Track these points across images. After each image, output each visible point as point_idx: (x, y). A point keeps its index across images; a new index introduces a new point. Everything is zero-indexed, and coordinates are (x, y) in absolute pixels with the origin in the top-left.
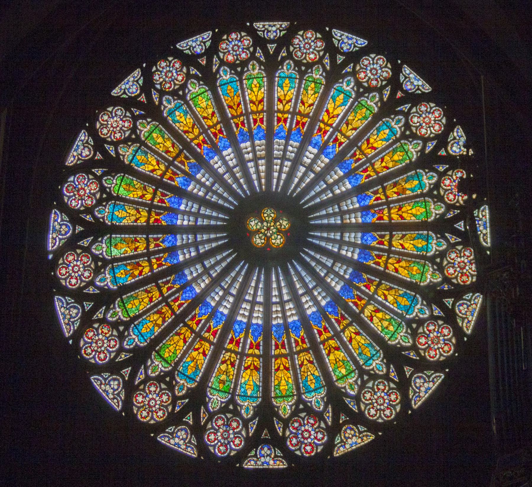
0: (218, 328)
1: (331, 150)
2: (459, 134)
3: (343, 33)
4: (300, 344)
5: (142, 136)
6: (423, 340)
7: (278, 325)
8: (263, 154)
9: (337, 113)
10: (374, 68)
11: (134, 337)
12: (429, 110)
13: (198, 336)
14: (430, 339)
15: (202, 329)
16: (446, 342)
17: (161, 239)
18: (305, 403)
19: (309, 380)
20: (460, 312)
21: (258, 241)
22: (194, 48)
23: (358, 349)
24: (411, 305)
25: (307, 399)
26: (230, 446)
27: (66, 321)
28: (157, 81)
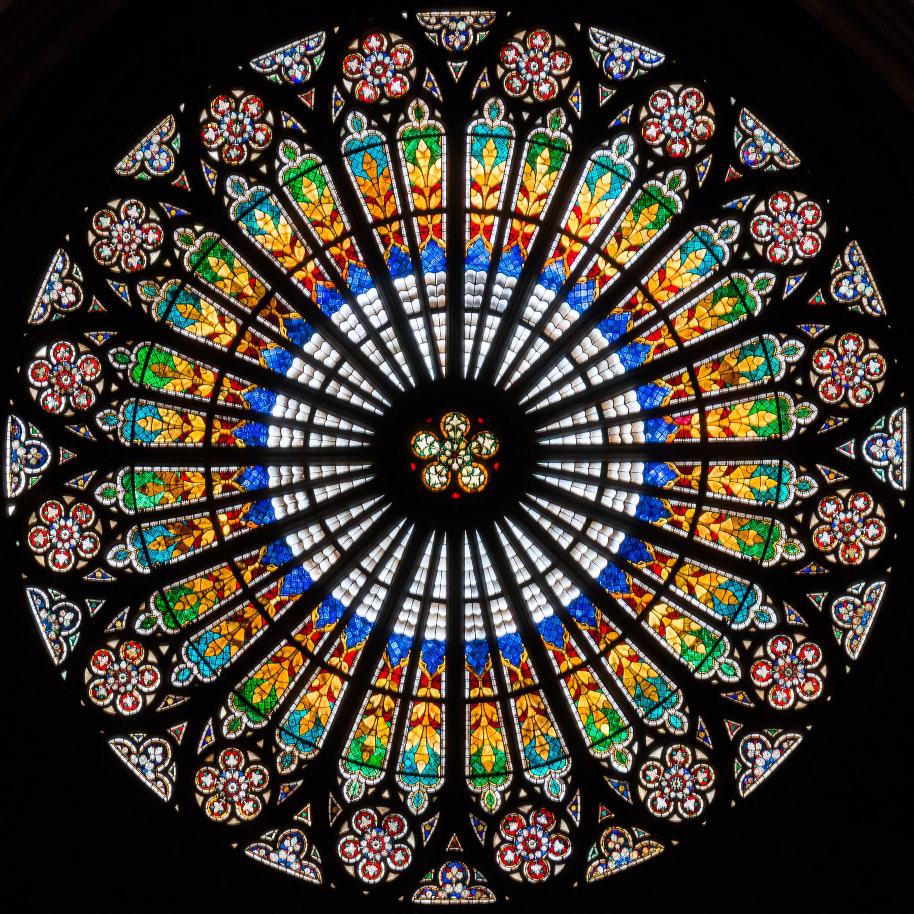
0: (358, 647)
1: (583, 293)
2: (855, 259)
3: (612, 36)
4: (521, 678)
5: (185, 262)
6: (763, 672)
7: (476, 643)
8: (442, 302)
9: (598, 214)
10: (677, 116)
11: (190, 665)
12: (792, 207)
13: (317, 662)
14: (777, 669)
15: (324, 650)
16: (809, 675)
17: (235, 476)
18: (529, 786)
19: (537, 744)
20: (840, 617)
22: (288, 69)
24: (741, 604)
25: (534, 781)
27: (53, 635)
28: (212, 142)
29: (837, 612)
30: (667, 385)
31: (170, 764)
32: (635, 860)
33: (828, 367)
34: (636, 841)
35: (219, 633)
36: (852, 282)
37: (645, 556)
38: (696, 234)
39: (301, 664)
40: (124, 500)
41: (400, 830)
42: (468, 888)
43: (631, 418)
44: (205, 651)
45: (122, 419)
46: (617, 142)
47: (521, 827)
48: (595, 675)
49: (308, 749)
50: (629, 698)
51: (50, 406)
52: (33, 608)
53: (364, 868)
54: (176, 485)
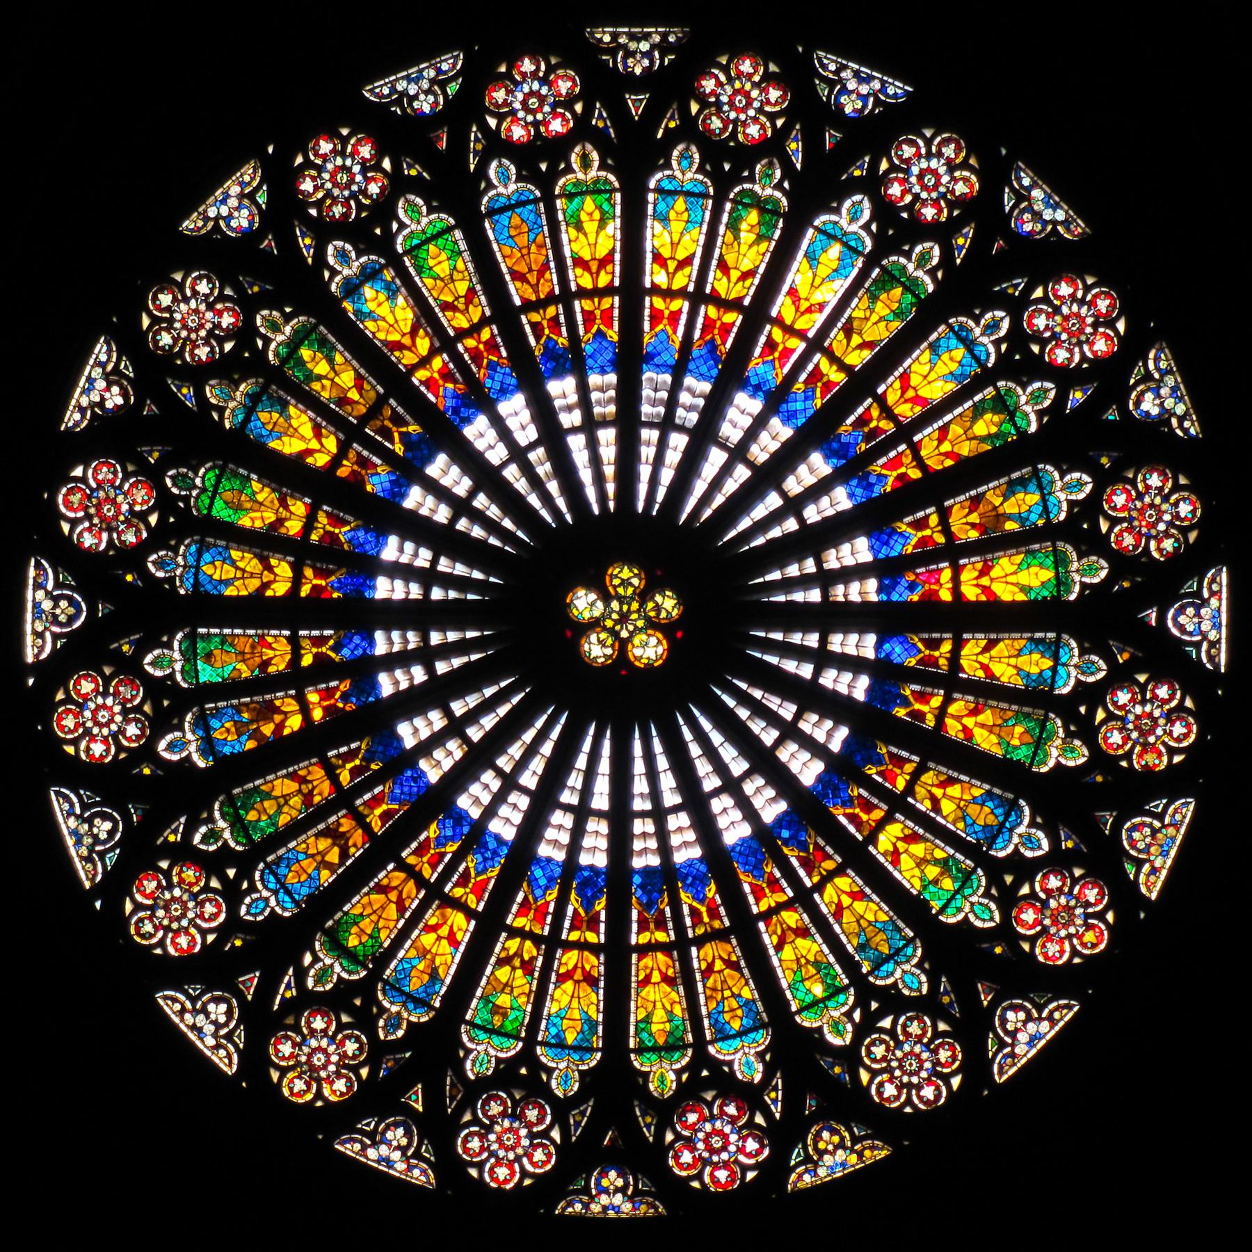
0: (489, 875)
1: (799, 406)
4: (706, 919)
5: (271, 356)
6: (1029, 916)
7: (647, 871)
9: (821, 300)
11: (265, 894)
12: (1080, 294)
13: (435, 894)
14: (1048, 913)
15: (445, 877)
16: (1090, 921)
17: (331, 642)
18: (715, 1064)
19: (726, 1009)
20: (1133, 844)
23: (858, 935)
24: (1002, 825)
25: (721, 1057)
27: (84, 851)
28: (310, 195)
29: (1130, 837)
30: (909, 530)
31: (237, 1027)
33: (1124, 508)
34: (855, 1140)
35: (305, 853)
36: (1158, 396)
37: (875, 757)
38: (951, 327)
39: (413, 895)
41: (541, 1120)
42: (631, 1199)
44: (286, 876)
45: (182, 563)
46: (848, 204)
47: (702, 1119)
48: (805, 916)
50: (850, 949)
51: (87, 545)
52: (59, 814)
53: (492, 1171)
54: (253, 653)
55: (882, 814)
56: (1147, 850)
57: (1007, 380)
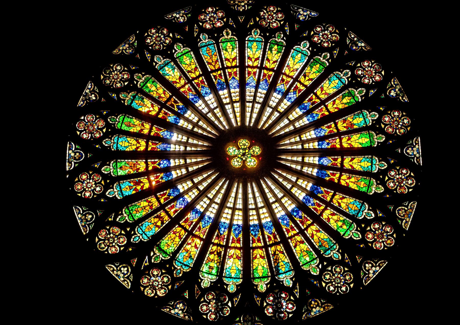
0: (207, 228)
1: (292, 96)
2: (396, 83)
7: (254, 226)
11: (139, 235)
12: (370, 65)
13: (190, 234)
17: (157, 163)
21: (236, 163)
23: (319, 242)
26: (219, 314)
27: (83, 224)
28: (149, 43)
29: (398, 213)
30: (326, 128)
32: (322, 312)
35: (151, 223)
39: (184, 234)
40: (113, 172)
43: (312, 140)
48: (302, 237)
49: (187, 268)
50: (317, 247)
54: (134, 166)
55: (324, 207)
56: (404, 216)
57: (351, 88)
